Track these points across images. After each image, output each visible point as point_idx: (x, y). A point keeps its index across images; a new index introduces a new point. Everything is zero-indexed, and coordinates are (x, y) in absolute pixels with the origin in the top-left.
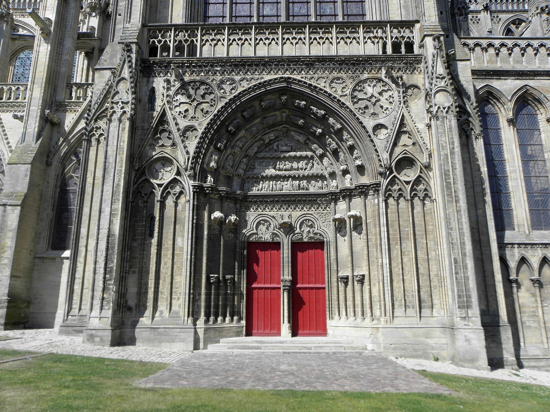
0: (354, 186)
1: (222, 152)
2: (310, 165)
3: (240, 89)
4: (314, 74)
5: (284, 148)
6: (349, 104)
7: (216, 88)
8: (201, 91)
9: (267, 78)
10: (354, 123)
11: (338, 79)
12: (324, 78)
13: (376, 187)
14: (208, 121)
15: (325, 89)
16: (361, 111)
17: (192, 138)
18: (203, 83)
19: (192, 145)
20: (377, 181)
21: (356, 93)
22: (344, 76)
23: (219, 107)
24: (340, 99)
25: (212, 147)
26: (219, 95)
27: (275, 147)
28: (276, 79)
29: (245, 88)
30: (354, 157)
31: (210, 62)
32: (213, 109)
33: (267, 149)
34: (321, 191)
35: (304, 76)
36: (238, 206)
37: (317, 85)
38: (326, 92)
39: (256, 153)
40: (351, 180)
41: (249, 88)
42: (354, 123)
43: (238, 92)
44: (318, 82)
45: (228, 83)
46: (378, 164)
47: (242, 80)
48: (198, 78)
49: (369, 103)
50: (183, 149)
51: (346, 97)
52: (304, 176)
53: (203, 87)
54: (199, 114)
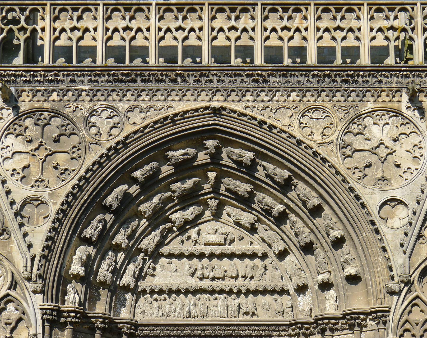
3: (129, 129)
4: (270, 100)
6: (335, 159)
7: (81, 126)
8: (53, 130)
9: (181, 107)
11: (316, 109)
13: (381, 315)
14: (68, 188)
15: (289, 131)
16: (358, 174)
18: (56, 113)
19: (39, 234)
21: (348, 139)
22: (329, 105)
23: (89, 162)
26: (88, 139)
29: (137, 128)
30: (342, 260)
32: (76, 165)
35: (250, 104)
37: (275, 124)
38: (291, 136)
41: (145, 127)
43: (125, 134)
45: (105, 114)
46: (387, 273)
47: (131, 110)
48: (47, 105)
49: (374, 159)
50: (22, 240)
51: (330, 147)
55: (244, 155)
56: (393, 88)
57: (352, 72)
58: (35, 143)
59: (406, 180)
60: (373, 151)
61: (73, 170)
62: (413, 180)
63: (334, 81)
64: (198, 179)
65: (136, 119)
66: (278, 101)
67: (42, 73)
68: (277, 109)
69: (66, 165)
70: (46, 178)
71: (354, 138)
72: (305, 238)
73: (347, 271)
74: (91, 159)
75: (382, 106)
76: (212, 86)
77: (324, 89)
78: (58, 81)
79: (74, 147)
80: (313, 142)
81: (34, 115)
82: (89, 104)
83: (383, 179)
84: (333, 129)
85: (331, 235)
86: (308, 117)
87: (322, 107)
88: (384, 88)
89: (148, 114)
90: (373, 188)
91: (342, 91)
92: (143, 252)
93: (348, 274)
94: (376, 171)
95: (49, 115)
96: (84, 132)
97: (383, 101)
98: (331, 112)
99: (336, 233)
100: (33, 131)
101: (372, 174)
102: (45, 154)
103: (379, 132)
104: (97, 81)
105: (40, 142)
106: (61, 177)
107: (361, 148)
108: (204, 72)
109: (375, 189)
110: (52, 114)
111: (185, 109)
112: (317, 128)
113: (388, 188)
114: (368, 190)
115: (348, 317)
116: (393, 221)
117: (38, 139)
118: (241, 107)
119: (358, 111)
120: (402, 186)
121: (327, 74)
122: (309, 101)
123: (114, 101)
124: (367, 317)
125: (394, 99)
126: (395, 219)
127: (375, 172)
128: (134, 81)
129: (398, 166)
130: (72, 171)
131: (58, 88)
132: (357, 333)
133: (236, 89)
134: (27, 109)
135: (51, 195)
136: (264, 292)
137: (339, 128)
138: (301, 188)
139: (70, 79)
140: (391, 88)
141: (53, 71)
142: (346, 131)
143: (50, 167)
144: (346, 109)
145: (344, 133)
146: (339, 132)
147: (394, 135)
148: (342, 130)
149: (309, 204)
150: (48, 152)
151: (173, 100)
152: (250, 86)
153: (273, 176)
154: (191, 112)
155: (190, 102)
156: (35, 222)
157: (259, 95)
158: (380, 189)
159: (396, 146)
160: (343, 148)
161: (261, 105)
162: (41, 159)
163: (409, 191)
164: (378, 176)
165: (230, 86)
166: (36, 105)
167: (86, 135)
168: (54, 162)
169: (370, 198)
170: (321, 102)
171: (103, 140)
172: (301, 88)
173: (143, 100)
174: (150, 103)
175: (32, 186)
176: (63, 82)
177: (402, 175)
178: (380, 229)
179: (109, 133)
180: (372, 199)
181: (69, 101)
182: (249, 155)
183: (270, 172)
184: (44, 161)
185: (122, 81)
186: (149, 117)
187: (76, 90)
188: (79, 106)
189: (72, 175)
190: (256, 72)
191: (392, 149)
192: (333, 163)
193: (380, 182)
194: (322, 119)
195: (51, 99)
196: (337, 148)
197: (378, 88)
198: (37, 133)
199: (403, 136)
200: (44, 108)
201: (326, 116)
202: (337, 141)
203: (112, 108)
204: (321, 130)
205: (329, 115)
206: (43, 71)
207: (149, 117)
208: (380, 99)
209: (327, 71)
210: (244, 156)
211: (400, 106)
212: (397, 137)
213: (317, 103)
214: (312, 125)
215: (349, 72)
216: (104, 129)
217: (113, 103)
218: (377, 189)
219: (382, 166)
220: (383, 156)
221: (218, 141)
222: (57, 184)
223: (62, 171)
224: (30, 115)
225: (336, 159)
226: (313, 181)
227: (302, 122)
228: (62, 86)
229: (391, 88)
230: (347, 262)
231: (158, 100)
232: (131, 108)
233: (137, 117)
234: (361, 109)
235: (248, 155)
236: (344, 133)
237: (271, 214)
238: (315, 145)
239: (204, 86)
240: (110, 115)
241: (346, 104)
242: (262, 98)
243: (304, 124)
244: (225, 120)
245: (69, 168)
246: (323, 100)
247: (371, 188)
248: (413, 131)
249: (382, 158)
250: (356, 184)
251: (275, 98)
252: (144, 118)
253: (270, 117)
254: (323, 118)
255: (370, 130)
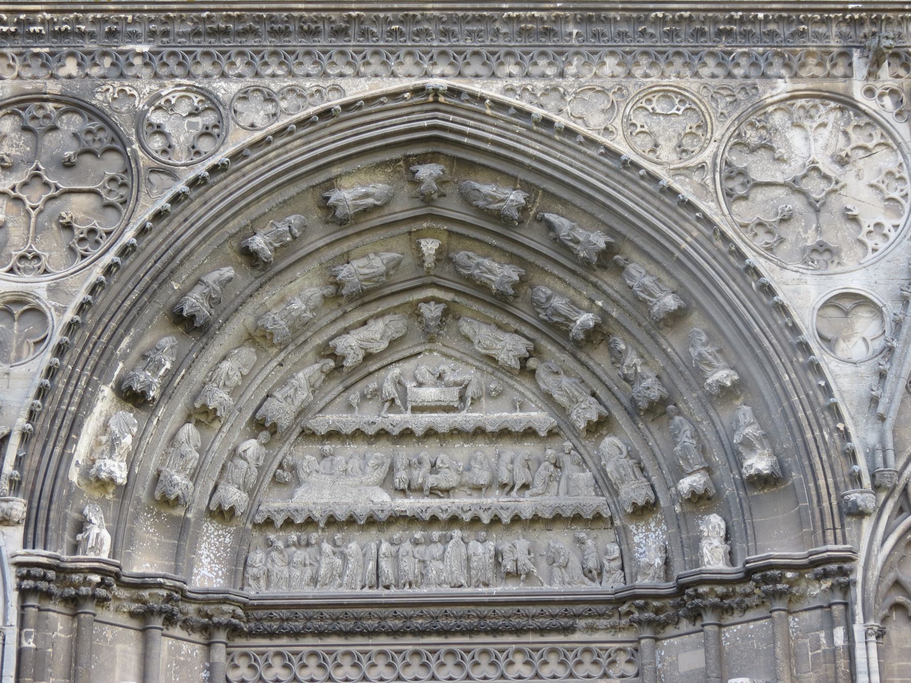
0: (739, 566)
1: (153, 412)
2: (546, 469)
3: (239, 139)
5: (430, 394)
9: (357, 89)
10: (732, 289)
12: (604, 91)
14: (97, 273)
16: (764, 238)
17: (19, 349)
18: (74, 105)
20: (833, 548)
21: (740, 160)
22: (691, 85)
23: (144, 215)
24: (676, 186)
25: (107, 391)
27: (389, 389)
28: (395, 95)
29: (258, 135)
30: (737, 439)
31: (105, 21)
33: (354, 396)
34: (594, 587)
35: (516, 83)
36: (219, 654)
37: (572, 125)
38: (611, 153)
39: (302, 412)
40: (727, 539)
42: (732, 289)
43: (230, 149)
44: (579, 109)
47: (244, 96)
48: (54, 88)
49: (796, 203)
51: (697, 177)
52: (516, 519)
53: (73, 123)
54: (52, 248)
55: (503, 196)
56: (831, 49)
57: (740, 13)
58: (23, 170)
59: (874, 250)
60: (794, 186)
61: (108, 233)
62: (889, 250)
63: (701, 33)
64: (396, 255)
65: (257, 117)
66: (577, 76)
67: (48, 16)
68: (576, 93)
69: (91, 222)
70: (44, 251)
71: (750, 158)
72: (648, 388)
73: (751, 466)
74: (150, 206)
75: (810, 86)
76: (429, 44)
77: (680, 49)
78: (82, 34)
79: (113, 180)
80: (659, 167)
81: (24, 109)
82: (150, 84)
83: (822, 249)
84: (703, 138)
85: (709, 381)
86: (645, 113)
87: (676, 89)
88: (811, 49)
89: (284, 104)
90: (801, 270)
91: (720, 54)
92: (266, 429)
93: (752, 472)
94: (806, 232)
95: (56, 108)
96: (136, 146)
97: (813, 77)
98: (697, 101)
99: (722, 375)
100: (18, 146)
101: (797, 239)
102: (44, 197)
103: (809, 142)
104: (166, 33)
105: (33, 170)
106: (79, 249)
107: (768, 180)
108: (411, 13)
109: (804, 271)
110: (64, 107)
111: (368, 93)
112: (668, 135)
113: (833, 268)
114: (789, 275)
115: (757, 576)
116: (850, 344)
117: (30, 162)
118: (494, 89)
119: (757, 99)
120: (865, 264)
121: (686, 18)
122: (647, 76)
123: (207, 76)
124: (801, 576)
125: (840, 71)
126: (854, 340)
127: (802, 233)
128: (253, 32)
129: (854, 219)
130: (104, 235)
131: (81, 49)
132: (780, 616)
133: (484, 51)
134: (7, 96)
135: (53, 290)
136: (557, 519)
137: (717, 135)
138: (634, 272)
139: (110, 29)
140: (827, 49)
141: (71, 11)
142: (733, 141)
143: (54, 226)
144: (729, 92)
145: (728, 147)
146: (716, 144)
147: (841, 150)
148: (725, 140)
149: (656, 308)
150: (52, 193)
151: (342, 75)
152: (513, 44)
153: (571, 244)
154: (382, 99)
155: (379, 79)
156: (13, 354)
157: (536, 64)
158: (816, 272)
159: (848, 177)
160: (729, 178)
161: (540, 84)
162: (34, 208)
163: (884, 277)
164: (810, 243)
165: (469, 42)
166: (28, 86)
167: (140, 153)
168: (63, 214)
169: (794, 291)
170: (673, 79)
171: (180, 163)
172: (627, 49)
173: (274, 76)
174: (289, 82)
175: (11, 271)
176: (92, 35)
177: (865, 239)
178: (822, 364)
179: (193, 147)
180: (799, 293)
181: (104, 77)
182: (516, 197)
183: (563, 233)
184: (41, 212)
185: (226, 32)
186: (286, 112)
187: (122, 53)
188: (127, 89)
189: (105, 243)
190: (529, 14)
191: (837, 183)
192: (708, 212)
193: (815, 256)
194: (677, 115)
195: (62, 72)
196: (714, 179)
197: (798, 49)
198: (28, 149)
199: (861, 153)
200: (45, 94)
201: (687, 109)
202: (715, 164)
203: (200, 91)
204: (675, 142)
205: (694, 106)
206: (48, 11)
207: (286, 112)
208: (803, 73)
209: (686, 10)
210: (502, 200)
211: (849, 88)
212: (847, 155)
213: (665, 81)
214: (655, 129)
215: (733, 13)
216: (182, 139)
217: (205, 81)
218: (809, 272)
219: (818, 219)
220: (818, 197)
221: (443, 167)
222: (68, 265)
223: (81, 236)
224: (15, 108)
225: (713, 205)
226: (663, 253)
227: (634, 121)
228: (90, 46)
229: (827, 49)
230: (748, 444)
231: (308, 75)
232: (246, 92)
233: (258, 112)
234: (764, 92)
235: (512, 197)
236: (728, 147)
237: (567, 332)
238: (664, 172)
239: (409, 44)
240: (197, 109)
241: (733, 83)
242: (542, 69)
243: (639, 125)
244: (458, 119)
245: (98, 227)
246: (675, 77)
247: (795, 269)
248: (882, 141)
249: (817, 201)
250: (762, 260)
251: (571, 70)
252: (274, 115)
253: (560, 111)
254: (680, 113)
255: (787, 140)
